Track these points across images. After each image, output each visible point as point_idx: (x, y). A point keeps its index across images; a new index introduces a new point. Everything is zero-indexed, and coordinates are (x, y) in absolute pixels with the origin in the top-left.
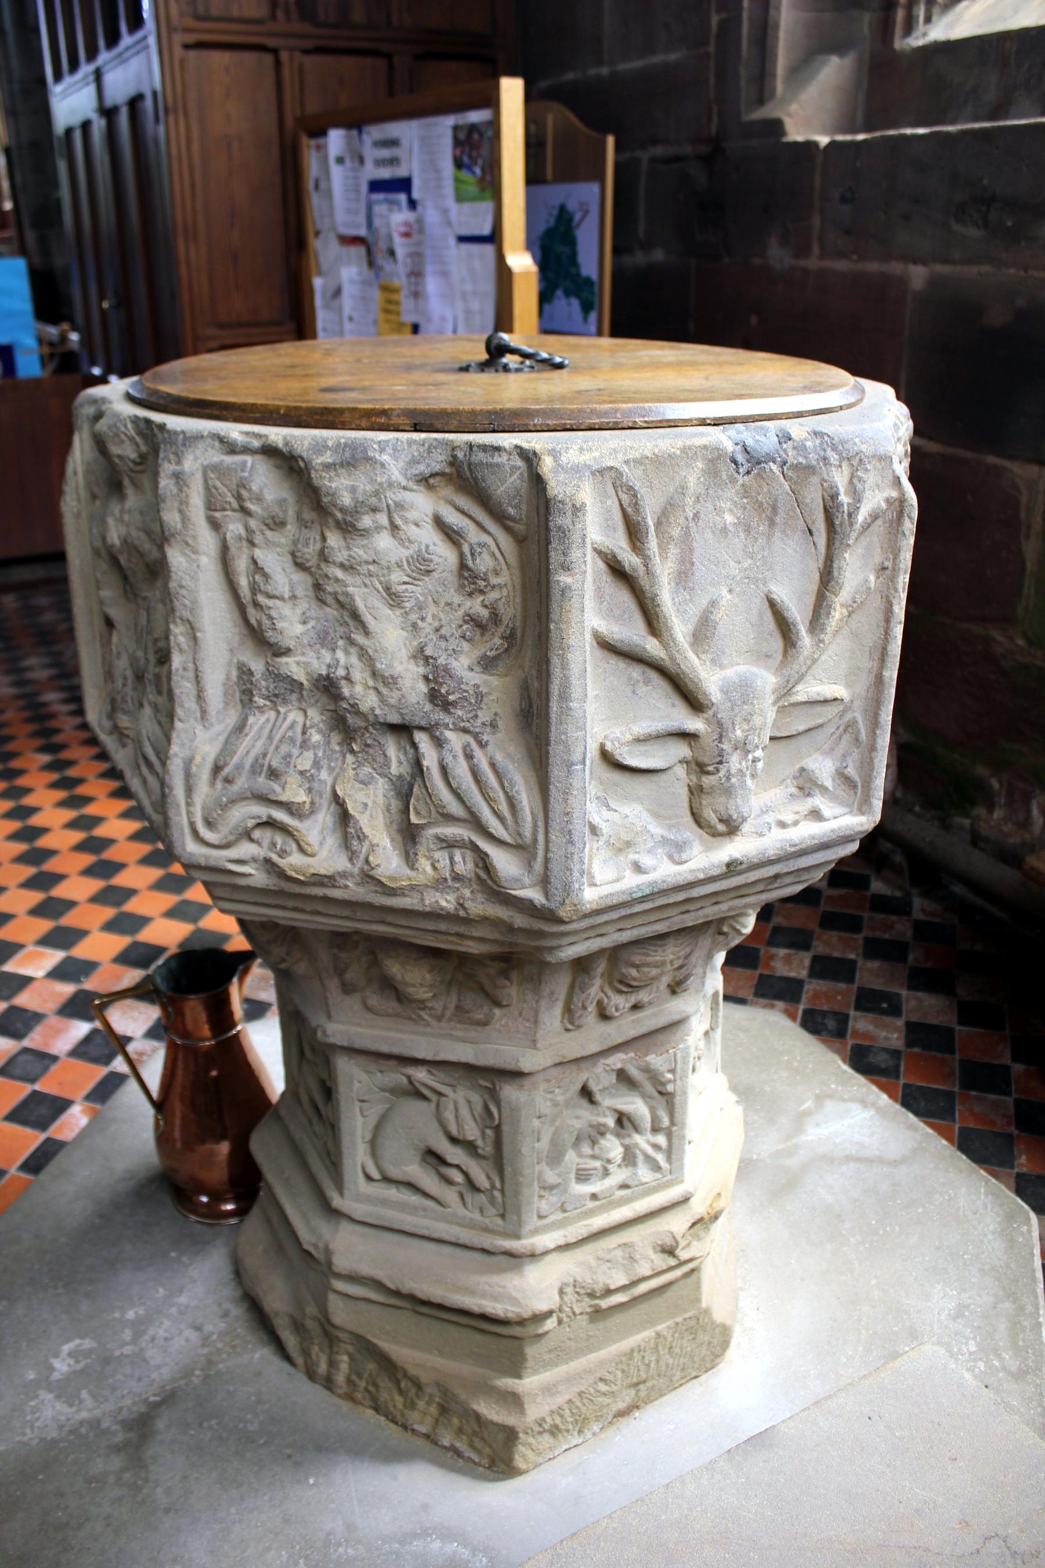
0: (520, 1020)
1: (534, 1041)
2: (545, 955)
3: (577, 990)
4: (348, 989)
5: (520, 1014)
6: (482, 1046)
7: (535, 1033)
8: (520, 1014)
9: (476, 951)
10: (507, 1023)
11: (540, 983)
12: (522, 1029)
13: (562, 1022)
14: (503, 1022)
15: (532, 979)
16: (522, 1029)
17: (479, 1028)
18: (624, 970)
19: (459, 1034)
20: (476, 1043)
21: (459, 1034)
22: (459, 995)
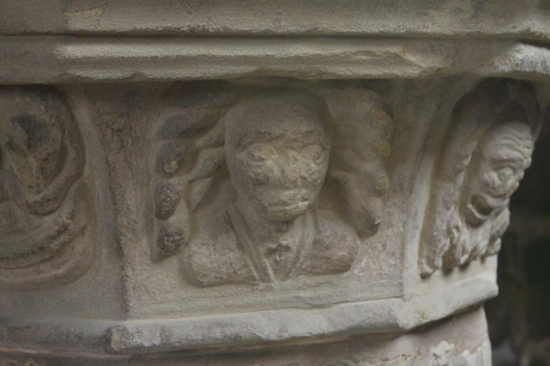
0: (383, 256)
1: (401, 284)
2: (497, 63)
3: (440, 208)
4: (167, 248)
5: (384, 246)
6: (336, 309)
7: (402, 272)
8: (384, 246)
9: (412, 72)
10: (367, 264)
11: (411, 192)
12: (386, 269)
13: (420, 263)
14: (363, 264)
15: (402, 189)
16: (386, 269)
17: (333, 278)
18: (486, 176)
19: (307, 294)
20: (330, 305)
21: (307, 294)
22: (316, 224)
